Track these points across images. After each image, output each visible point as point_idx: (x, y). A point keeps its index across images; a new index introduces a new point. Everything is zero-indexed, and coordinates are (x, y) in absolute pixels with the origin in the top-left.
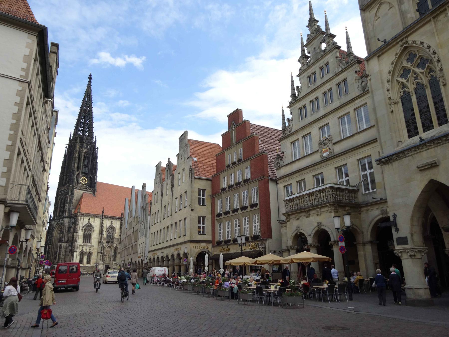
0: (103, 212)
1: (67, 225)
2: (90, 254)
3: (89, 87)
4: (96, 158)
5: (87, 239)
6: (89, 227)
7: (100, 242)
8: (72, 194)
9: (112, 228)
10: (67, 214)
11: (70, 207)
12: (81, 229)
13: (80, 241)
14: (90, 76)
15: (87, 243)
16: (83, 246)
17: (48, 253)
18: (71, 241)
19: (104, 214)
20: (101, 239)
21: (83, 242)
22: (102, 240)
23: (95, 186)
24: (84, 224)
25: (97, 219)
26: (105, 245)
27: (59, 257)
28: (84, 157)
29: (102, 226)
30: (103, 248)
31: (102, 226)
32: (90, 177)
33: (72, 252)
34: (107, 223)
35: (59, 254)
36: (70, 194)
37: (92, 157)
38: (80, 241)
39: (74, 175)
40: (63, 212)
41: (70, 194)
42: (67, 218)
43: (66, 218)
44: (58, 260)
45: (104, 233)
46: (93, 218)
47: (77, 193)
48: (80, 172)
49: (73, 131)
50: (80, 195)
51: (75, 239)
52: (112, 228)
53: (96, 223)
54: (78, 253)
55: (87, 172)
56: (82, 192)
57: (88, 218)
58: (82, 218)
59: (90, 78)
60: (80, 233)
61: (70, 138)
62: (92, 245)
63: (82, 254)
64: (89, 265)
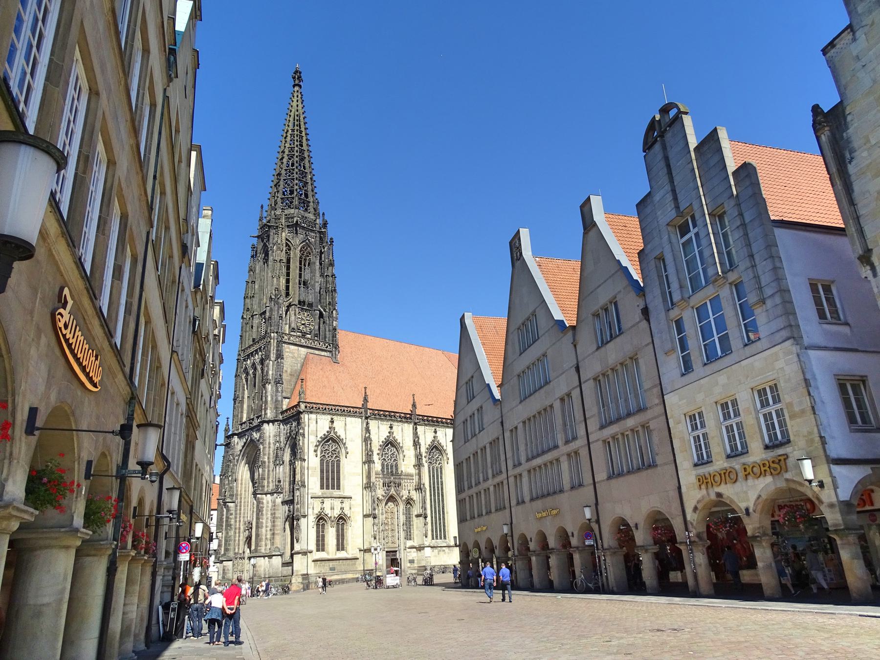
0: (366, 400)
1: (272, 442)
2: (342, 519)
4: (332, 264)
5: (331, 477)
7: (368, 486)
8: (280, 356)
9: (390, 443)
10: (269, 411)
11: (277, 391)
12: (312, 449)
15: (333, 488)
16: (323, 498)
17: (228, 525)
18: (286, 486)
19: (369, 406)
20: (369, 476)
21: (322, 487)
22: (373, 479)
23: (334, 336)
24: (321, 434)
25: (353, 419)
26: (380, 492)
27: (257, 535)
28: (300, 264)
29: (367, 440)
30: (375, 501)
31: (367, 440)
32: (321, 314)
34: (380, 431)
35: (257, 527)
36: (273, 356)
37: (321, 264)
39: (279, 307)
41: (273, 356)
42: (273, 422)
43: (268, 422)
44: (257, 545)
45: (376, 458)
46: (343, 418)
47: (293, 355)
48: (294, 299)
49: (266, 204)
50: (300, 360)
51: (298, 477)
52: (390, 443)
53: (350, 429)
54: (312, 519)
55: (310, 298)
56: (303, 351)
57: (329, 417)
58: (313, 416)
59: (297, 77)
60: (312, 462)
61: (261, 219)
62: (346, 494)
64: (342, 554)
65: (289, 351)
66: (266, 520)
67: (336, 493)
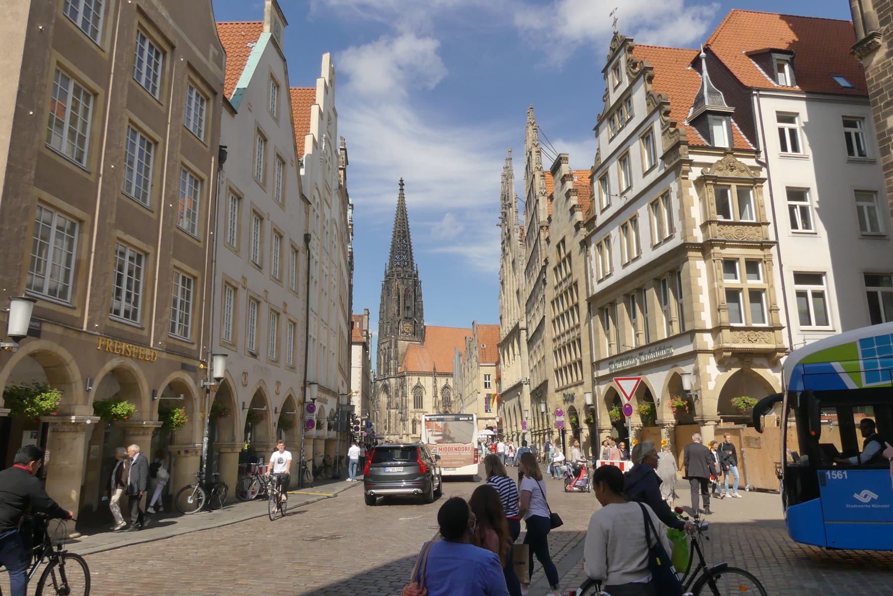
0: (435, 369)
3: (402, 197)
4: (421, 295)
5: (418, 403)
6: (418, 388)
8: (396, 346)
9: (446, 387)
13: (411, 406)
14: (401, 181)
16: (415, 412)
29: (435, 387)
31: (435, 387)
33: (403, 420)
34: (442, 382)
38: (411, 406)
40: (387, 370)
45: (439, 395)
47: (402, 345)
54: (410, 421)
60: (411, 397)
63: (414, 422)
65: (400, 343)
66: (393, 420)
67: (421, 410)
